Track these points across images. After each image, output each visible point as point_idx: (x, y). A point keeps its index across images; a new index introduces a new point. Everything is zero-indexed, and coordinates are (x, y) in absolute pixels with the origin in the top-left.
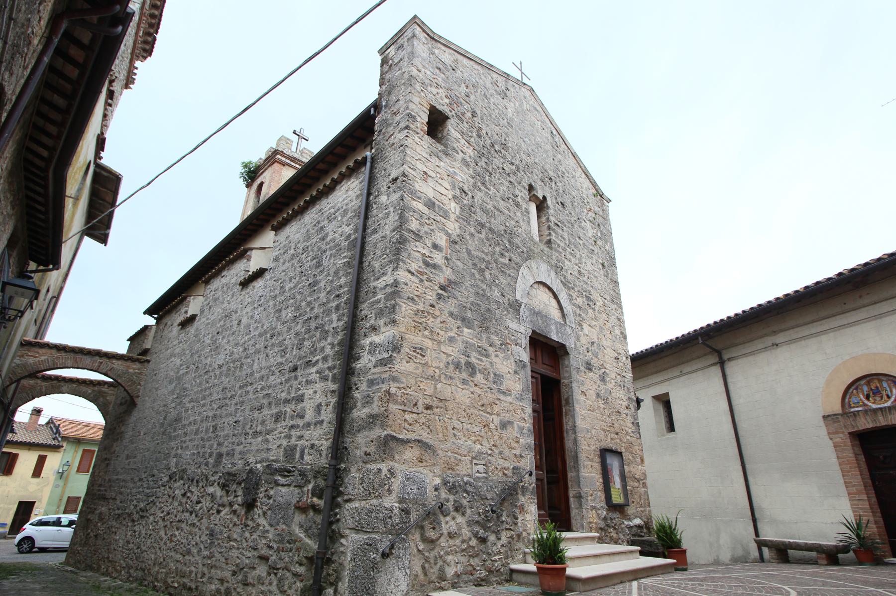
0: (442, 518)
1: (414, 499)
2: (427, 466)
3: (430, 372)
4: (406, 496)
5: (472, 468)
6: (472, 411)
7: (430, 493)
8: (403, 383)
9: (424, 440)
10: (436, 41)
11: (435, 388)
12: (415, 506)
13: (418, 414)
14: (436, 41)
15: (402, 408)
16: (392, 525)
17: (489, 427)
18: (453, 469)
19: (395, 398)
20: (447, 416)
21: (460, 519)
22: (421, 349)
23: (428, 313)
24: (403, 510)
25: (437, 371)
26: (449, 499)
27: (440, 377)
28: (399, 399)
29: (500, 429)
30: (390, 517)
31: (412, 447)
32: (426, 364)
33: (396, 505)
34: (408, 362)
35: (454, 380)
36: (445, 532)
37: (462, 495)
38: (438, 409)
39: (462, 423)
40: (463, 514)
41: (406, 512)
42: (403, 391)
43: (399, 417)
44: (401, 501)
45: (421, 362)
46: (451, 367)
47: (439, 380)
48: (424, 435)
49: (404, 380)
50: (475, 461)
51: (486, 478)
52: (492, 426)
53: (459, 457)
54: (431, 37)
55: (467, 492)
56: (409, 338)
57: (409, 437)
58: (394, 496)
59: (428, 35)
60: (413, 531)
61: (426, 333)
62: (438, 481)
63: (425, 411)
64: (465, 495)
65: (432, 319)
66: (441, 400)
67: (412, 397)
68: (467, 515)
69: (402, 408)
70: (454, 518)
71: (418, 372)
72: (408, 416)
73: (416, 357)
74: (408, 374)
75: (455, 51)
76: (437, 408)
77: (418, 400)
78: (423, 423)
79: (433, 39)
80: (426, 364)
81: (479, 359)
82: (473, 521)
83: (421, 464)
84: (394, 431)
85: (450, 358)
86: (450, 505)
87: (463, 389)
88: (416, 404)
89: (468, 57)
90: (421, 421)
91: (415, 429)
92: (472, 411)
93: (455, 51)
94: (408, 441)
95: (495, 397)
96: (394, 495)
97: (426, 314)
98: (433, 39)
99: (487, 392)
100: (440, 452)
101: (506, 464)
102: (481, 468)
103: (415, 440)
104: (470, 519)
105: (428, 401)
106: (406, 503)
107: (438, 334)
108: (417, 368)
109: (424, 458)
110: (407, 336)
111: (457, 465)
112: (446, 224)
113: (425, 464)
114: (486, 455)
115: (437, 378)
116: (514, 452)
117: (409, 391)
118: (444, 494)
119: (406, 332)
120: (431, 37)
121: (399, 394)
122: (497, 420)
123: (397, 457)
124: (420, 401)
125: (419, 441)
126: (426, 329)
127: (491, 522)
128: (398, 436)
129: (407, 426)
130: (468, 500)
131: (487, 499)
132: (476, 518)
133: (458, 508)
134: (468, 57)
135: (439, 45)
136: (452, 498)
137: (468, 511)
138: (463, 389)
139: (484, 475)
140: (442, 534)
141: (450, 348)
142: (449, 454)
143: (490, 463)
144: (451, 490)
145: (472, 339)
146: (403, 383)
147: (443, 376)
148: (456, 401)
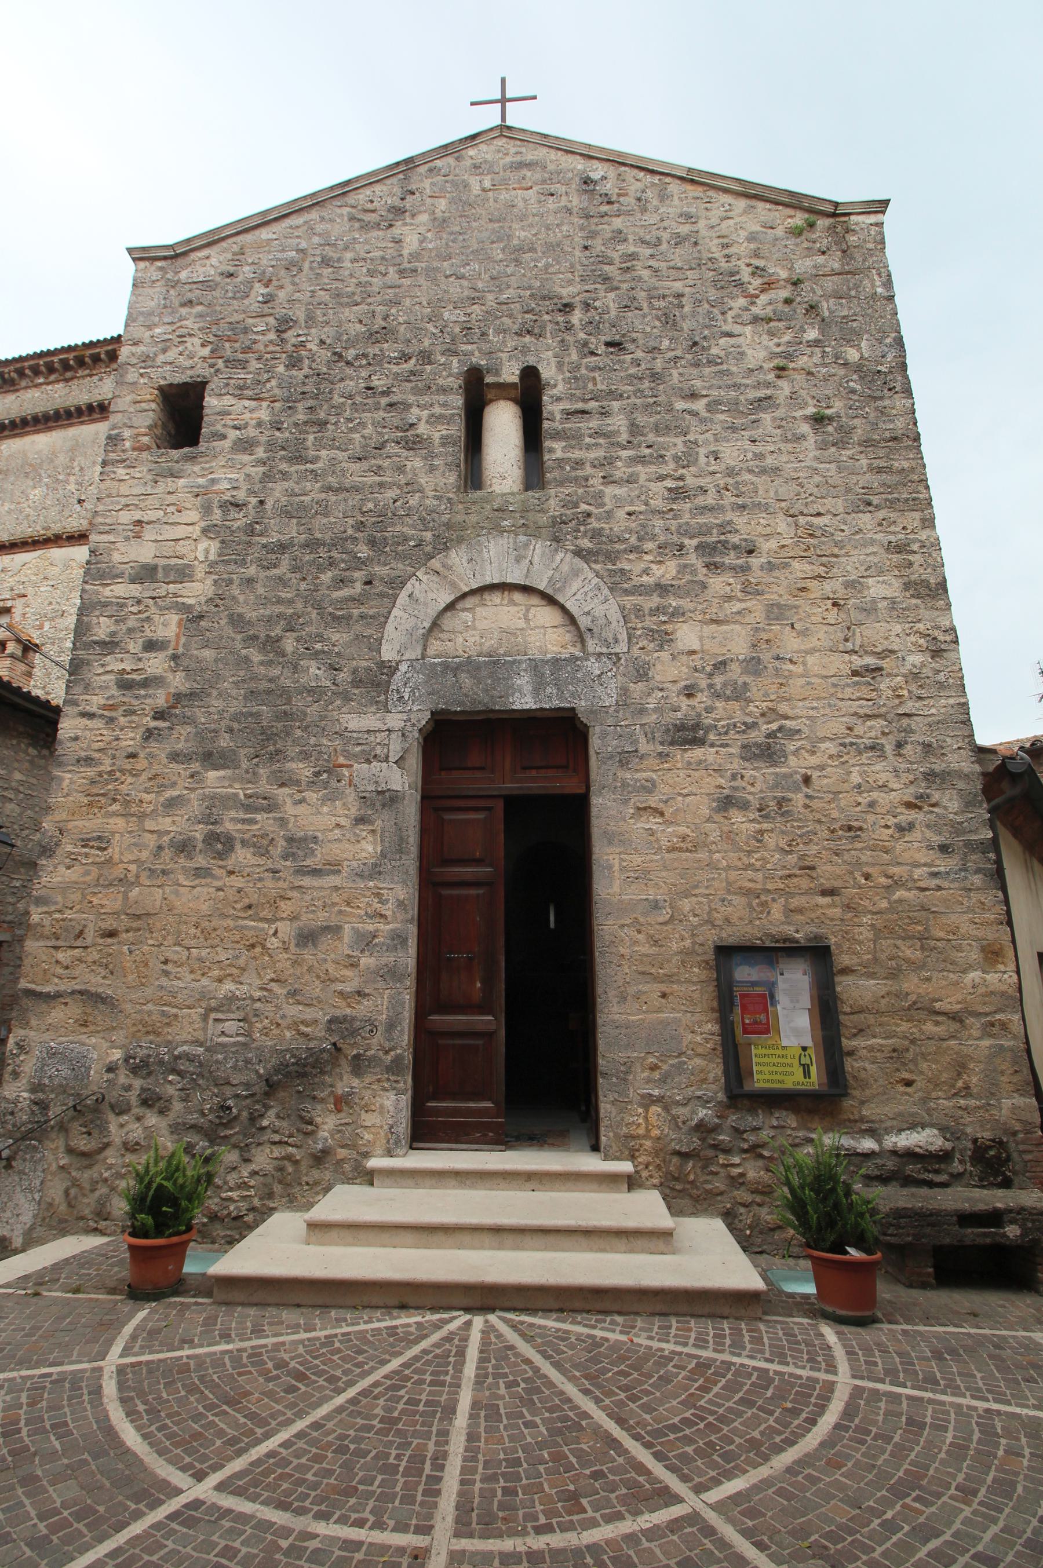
0: (111, 1117)
1: (61, 1085)
2: (98, 1032)
3: (118, 872)
4: (46, 1081)
5: (205, 1029)
6: (216, 922)
7: (96, 1074)
8: (56, 903)
9: (93, 990)
10: (185, 254)
11: (126, 896)
12: (61, 1097)
13: (86, 948)
14: (185, 254)
15: (53, 943)
16: (14, 1125)
17: (264, 947)
18: (158, 1034)
19: (39, 929)
20: (151, 942)
21: (152, 1119)
22: (99, 838)
23: (123, 771)
24: (36, 1103)
25: (133, 868)
26: (130, 1086)
27: (138, 877)
28: (47, 930)
29: (297, 945)
30: (12, 1113)
31: (66, 1004)
32: (109, 861)
33: (25, 1095)
34: (68, 868)
35: (172, 876)
36: (118, 1141)
37: (165, 1079)
38: (131, 934)
39: (188, 949)
40: (161, 1112)
41: (43, 1106)
42: (57, 916)
43: (44, 958)
44: (34, 1089)
45: (98, 860)
46: (167, 854)
47: (137, 883)
48: (97, 982)
49: (59, 899)
50: (213, 1015)
51: (245, 1044)
52: (273, 943)
53: (175, 1010)
54: (171, 258)
55: (179, 1073)
56: (76, 827)
57: (62, 988)
58: (23, 1082)
59: (165, 258)
60: (53, 1135)
61: (115, 807)
62: (117, 1055)
63: (101, 941)
64: (171, 1078)
65: (130, 780)
66: (138, 917)
67: (73, 923)
68: (172, 1115)
69: (53, 943)
70: (139, 1119)
71: (88, 878)
72: (60, 956)
73: (87, 855)
74: (65, 888)
75: (238, 233)
76: (127, 931)
77: (85, 926)
78: (94, 962)
79: (176, 256)
80: (109, 861)
81: (244, 821)
82: (184, 1124)
83: (84, 1030)
84: (33, 982)
85: (166, 839)
86: (133, 1097)
87: (194, 887)
88: (81, 932)
89: (276, 220)
90: (89, 959)
91: (77, 972)
92: (216, 922)
93: (238, 233)
94: (58, 995)
95: (285, 885)
96: (23, 1082)
97: (118, 774)
98: (176, 256)
99: (261, 879)
100: (128, 1007)
101: (309, 1014)
102: (231, 1027)
103: (73, 992)
104: (179, 1120)
105: (110, 924)
106: (44, 1092)
107: (141, 801)
108: (87, 873)
109: (90, 1019)
110: (70, 825)
111: (168, 1024)
112: (181, 593)
113: (92, 1028)
114: (248, 1002)
115: (133, 880)
116: (339, 987)
117: (69, 914)
118: (123, 1077)
119: (70, 818)
120: (171, 258)
121: (47, 922)
122: (286, 929)
123: (34, 1022)
124: (91, 926)
125: (81, 993)
126: (115, 800)
127: (232, 1128)
128: (39, 989)
129: (59, 971)
130: (179, 1086)
131: (228, 1083)
132: (193, 1118)
133: (149, 1101)
134: (276, 220)
135: (194, 256)
136: (138, 1083)
137: (177, 1106)
138: (194, 887)
139: (240, 1039)
140: (107, 1145)
141: (169, 820)
142: (150, 1007)
143: (256, 1015)
144: (135, 1070)
145: (230, 786)
146: (56, 903)
147: (144, 875)
148: (176, 912)
